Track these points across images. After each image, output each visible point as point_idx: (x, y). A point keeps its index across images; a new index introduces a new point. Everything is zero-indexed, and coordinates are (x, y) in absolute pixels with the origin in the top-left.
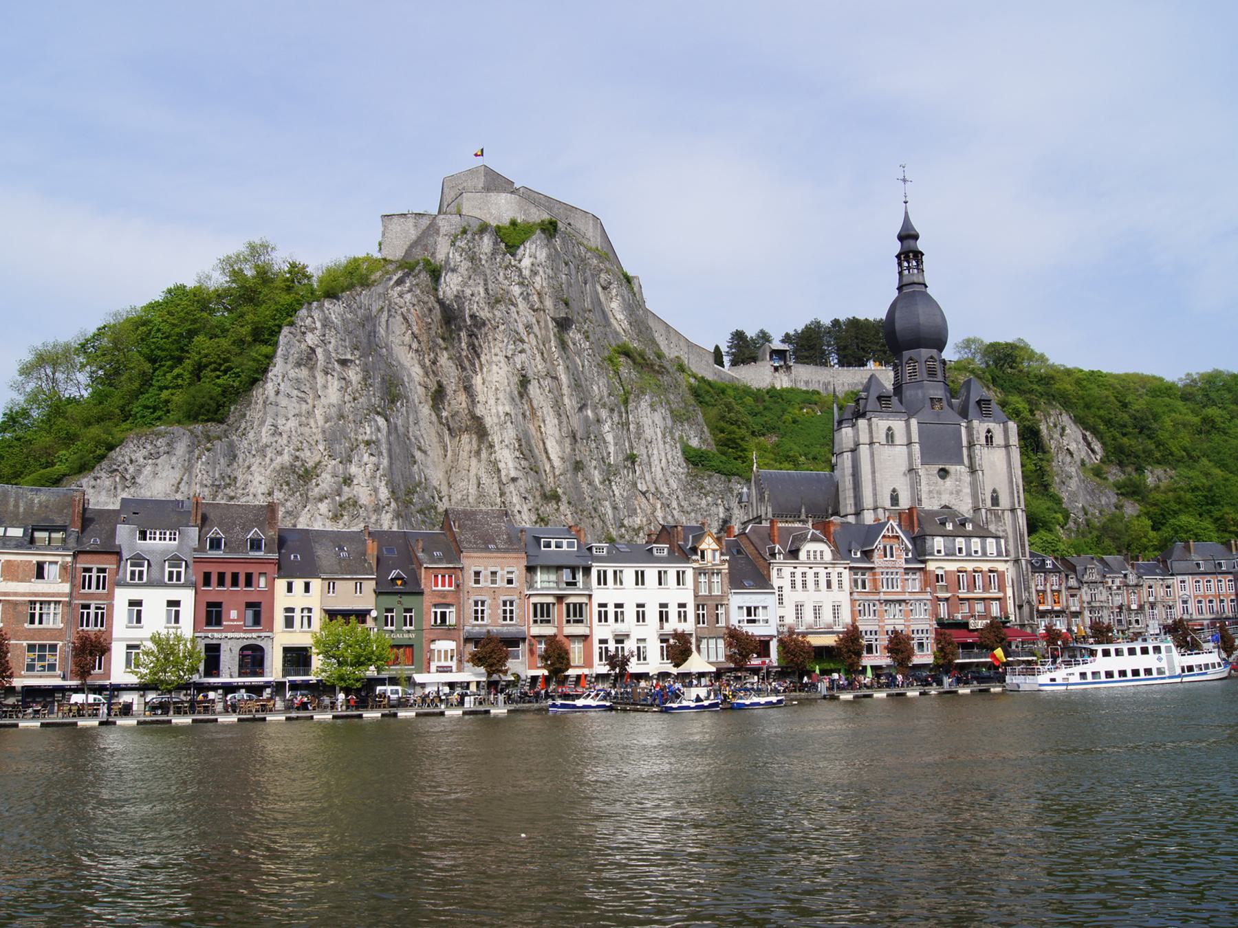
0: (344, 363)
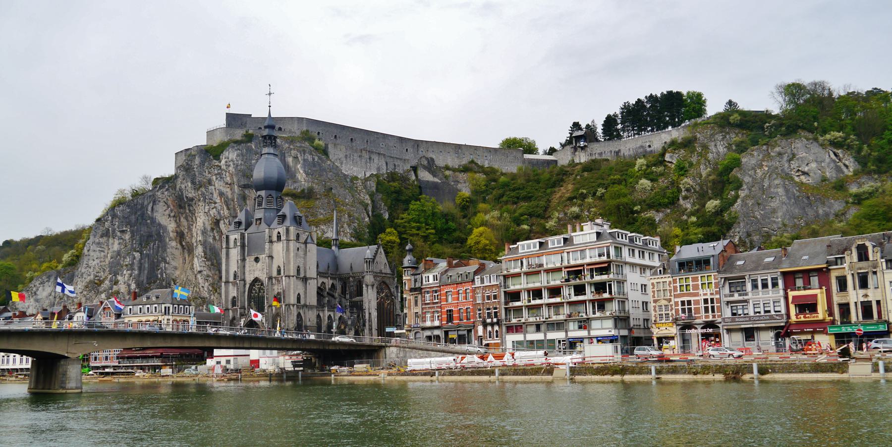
0: (123, 232)
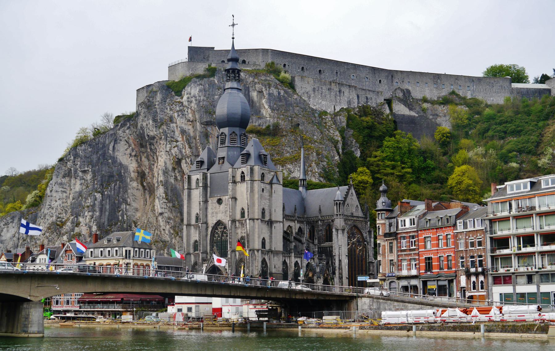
0: (84, 172)
